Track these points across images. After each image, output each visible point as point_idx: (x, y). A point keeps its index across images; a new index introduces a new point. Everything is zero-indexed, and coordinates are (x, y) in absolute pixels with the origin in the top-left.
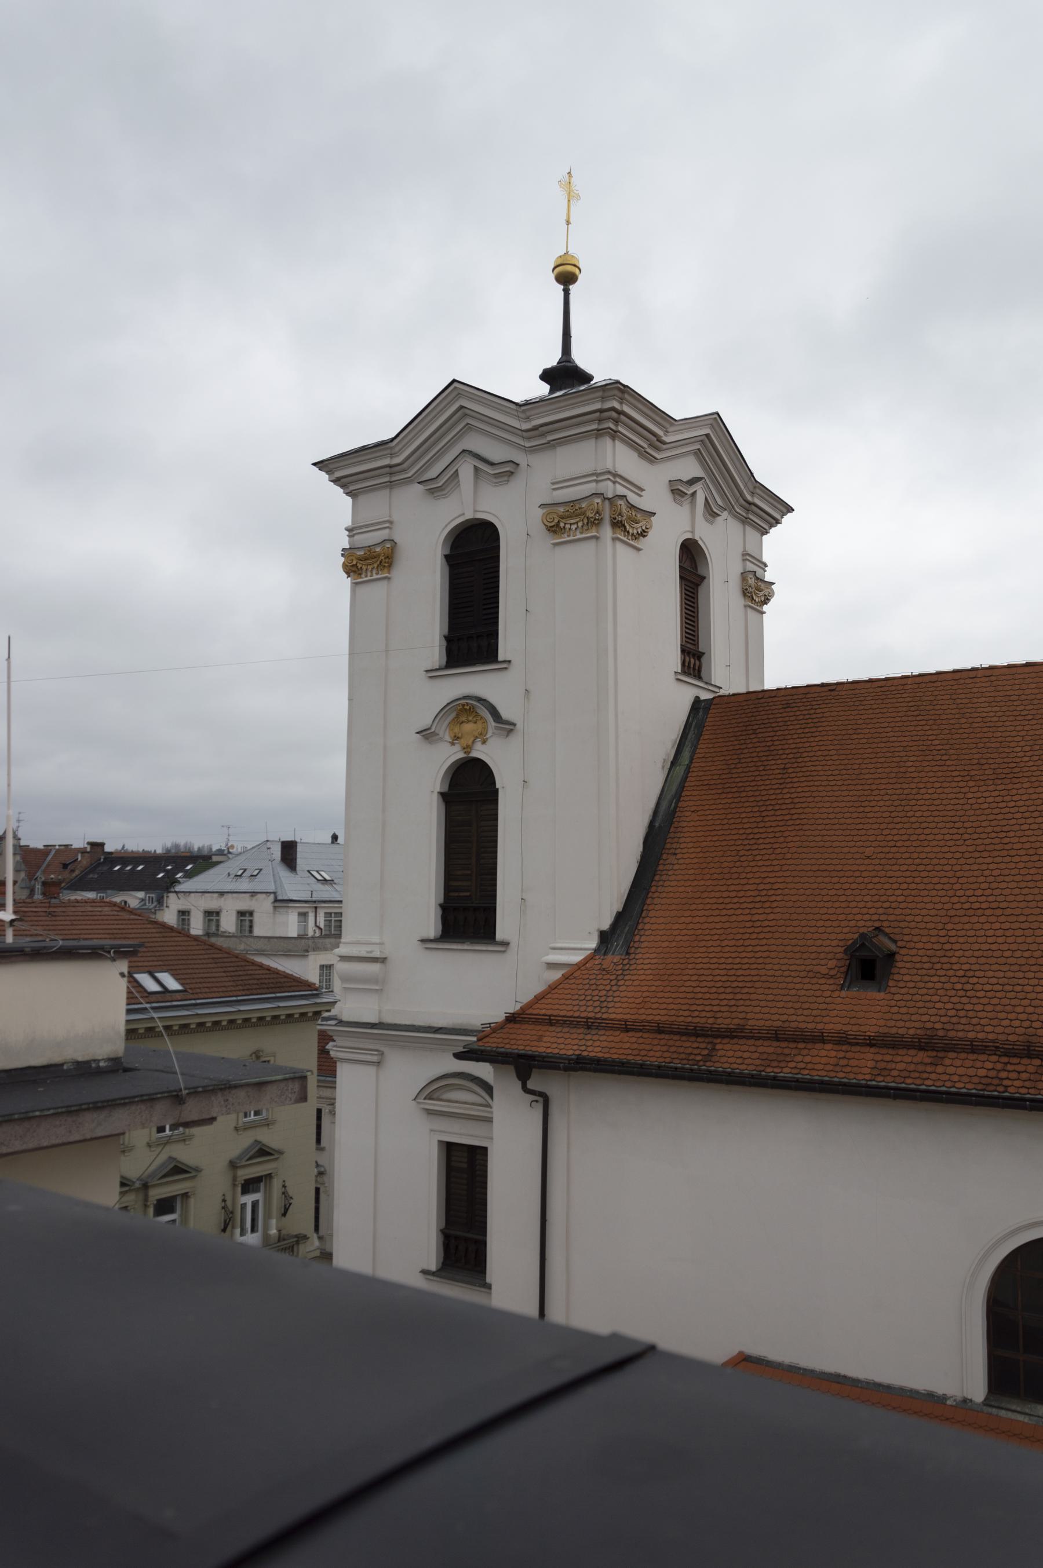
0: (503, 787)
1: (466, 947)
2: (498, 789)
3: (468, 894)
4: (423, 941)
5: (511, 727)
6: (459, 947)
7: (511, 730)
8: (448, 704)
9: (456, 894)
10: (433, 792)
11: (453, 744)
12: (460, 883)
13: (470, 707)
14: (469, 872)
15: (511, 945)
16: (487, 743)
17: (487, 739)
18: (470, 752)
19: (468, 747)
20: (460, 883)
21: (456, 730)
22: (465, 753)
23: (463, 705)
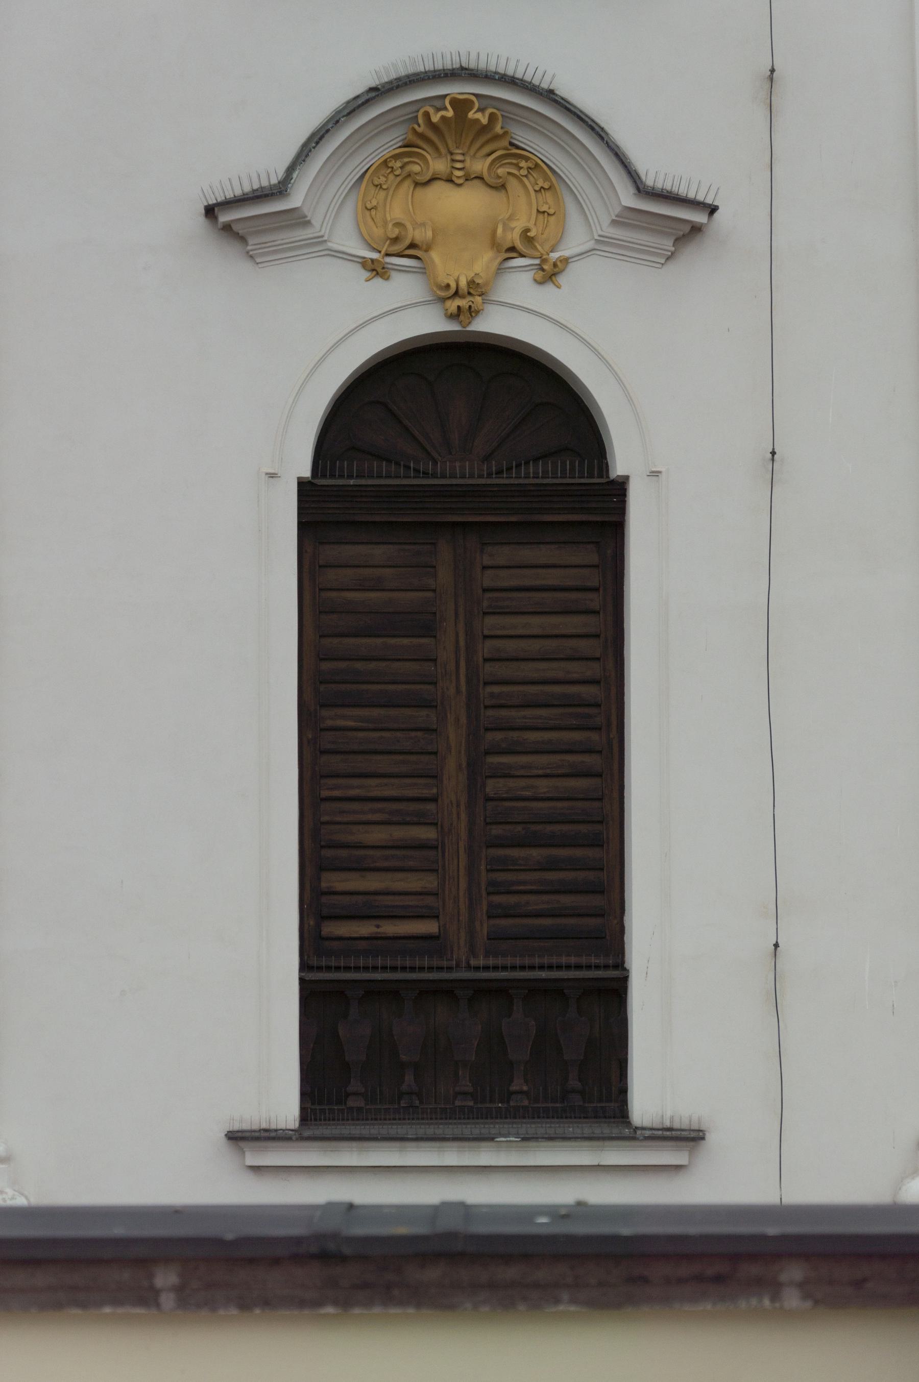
0: (655, 474)
1: (485, 1156)
2: (620, 488)
3: (429, 927)
4: (237, 1138)
5: (699, 218)
6: (451, 1156)
7: (696, 229)
8: (376, 93)
9: (365, 929)
10: (272, 476)
11: (377, 270)
12: (372, 882)
13: (492, 117)
14: (427, 834)
15: (711, 1138)
16: (562, 279)
17: (566, 261)
18: (473, 312)
19: (475, 288)
20: (372, 882)
21: (397, 210)
22: (454, 316)
23: (461, 105)
